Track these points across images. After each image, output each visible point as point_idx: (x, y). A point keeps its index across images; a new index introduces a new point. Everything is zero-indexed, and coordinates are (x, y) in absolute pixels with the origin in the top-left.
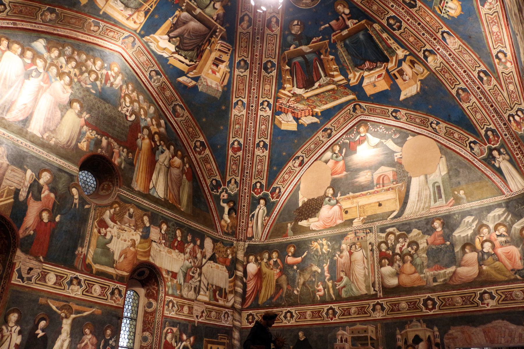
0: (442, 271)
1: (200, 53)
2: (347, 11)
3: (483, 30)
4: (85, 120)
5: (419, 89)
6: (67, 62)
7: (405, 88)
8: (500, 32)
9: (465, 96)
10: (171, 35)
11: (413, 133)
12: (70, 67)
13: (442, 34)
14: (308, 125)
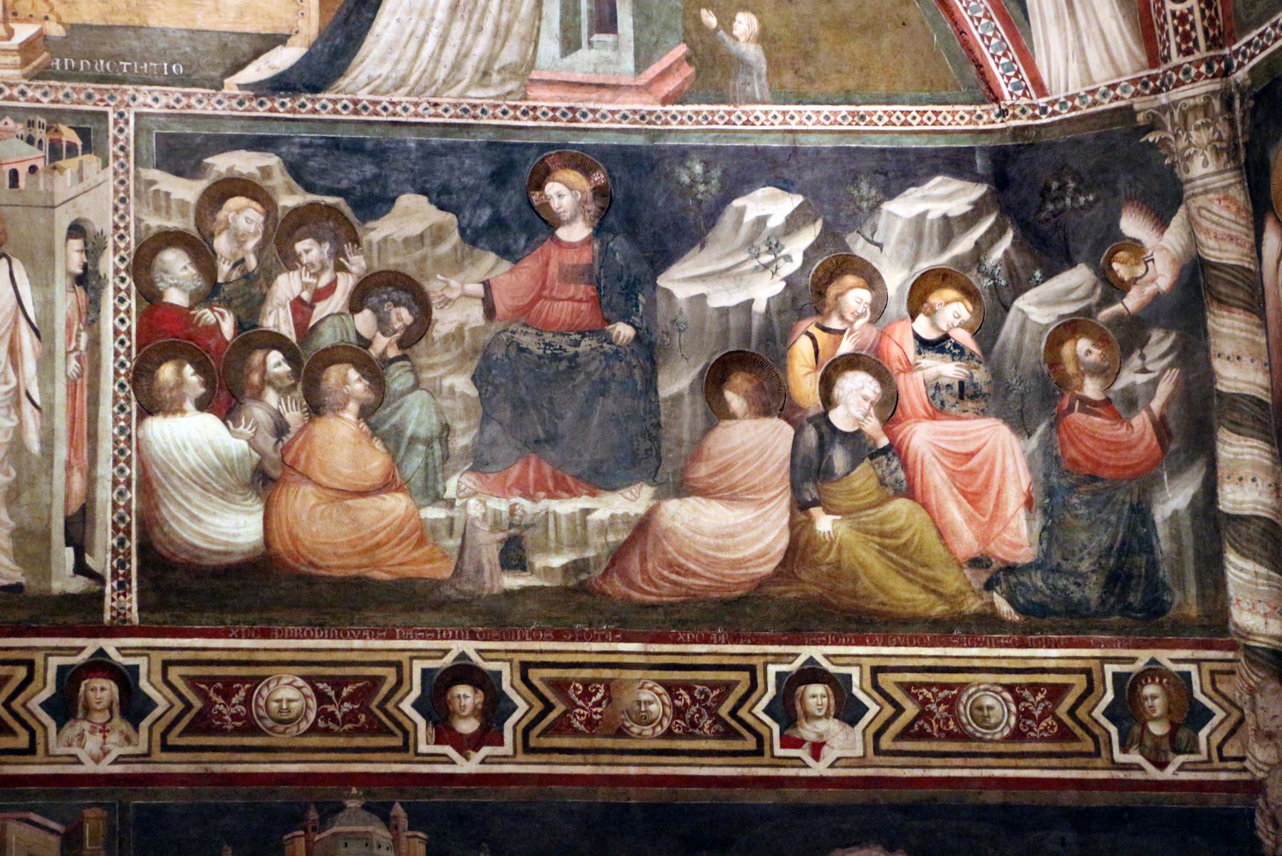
0: (566, 507)
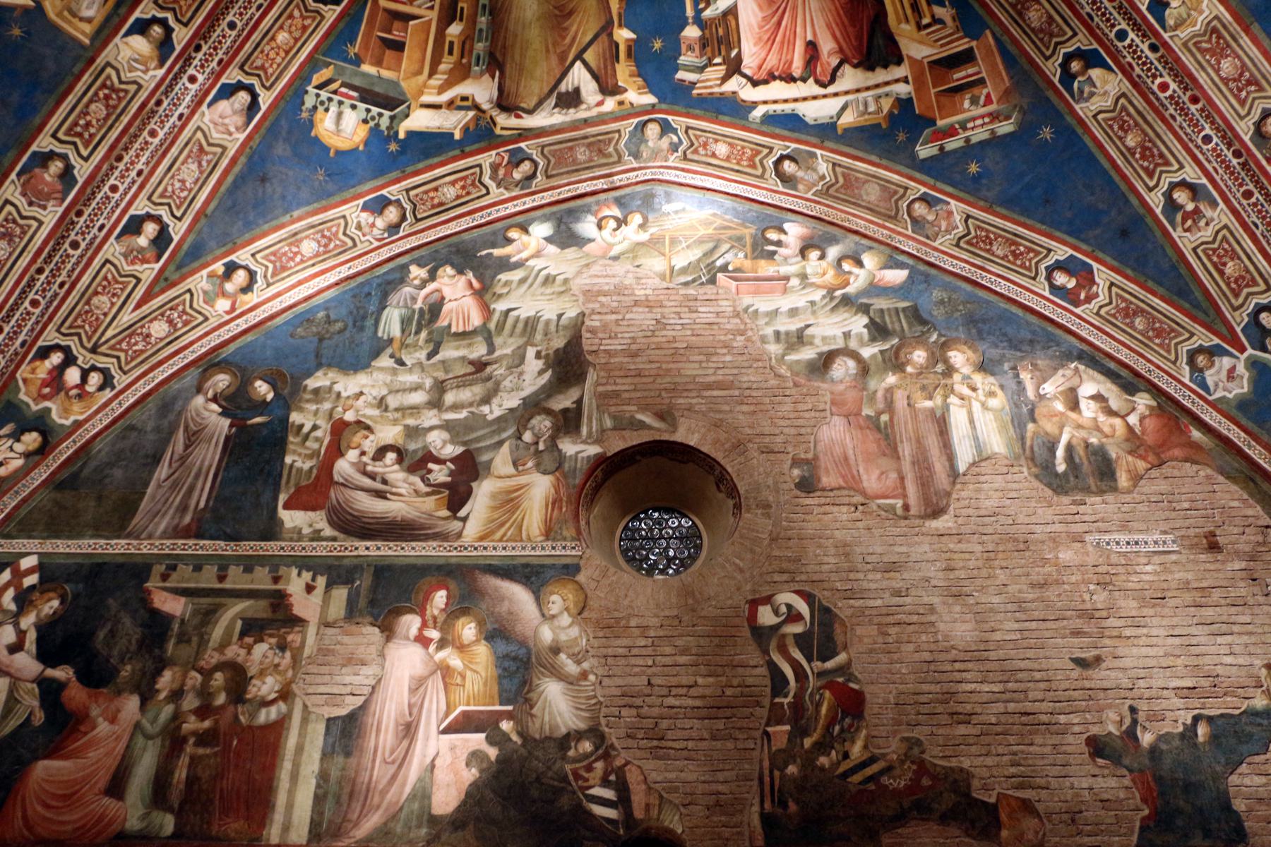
3: (296, 214)
8: (302, 261)
9: (47, 184)
13: (240, 86)
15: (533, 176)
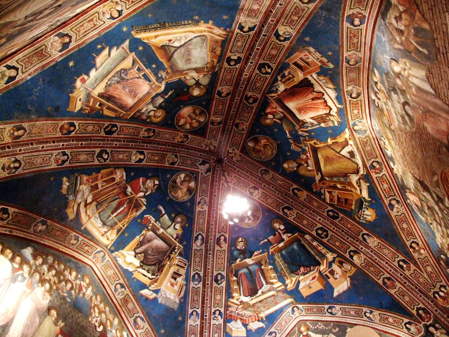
1: (161, 268)
2: (282, 227)
3: (395, 228)
4: (61, 329)
5: (349, 285)
6: (49, 270)
7: (337, 285)
8: (409, 228)
9: (390, 283)
10: (137, 251)
11: (351, 325)
12: (50, 275)
13: (363, 236)
14: (256, 330)
15: (377, 162)
